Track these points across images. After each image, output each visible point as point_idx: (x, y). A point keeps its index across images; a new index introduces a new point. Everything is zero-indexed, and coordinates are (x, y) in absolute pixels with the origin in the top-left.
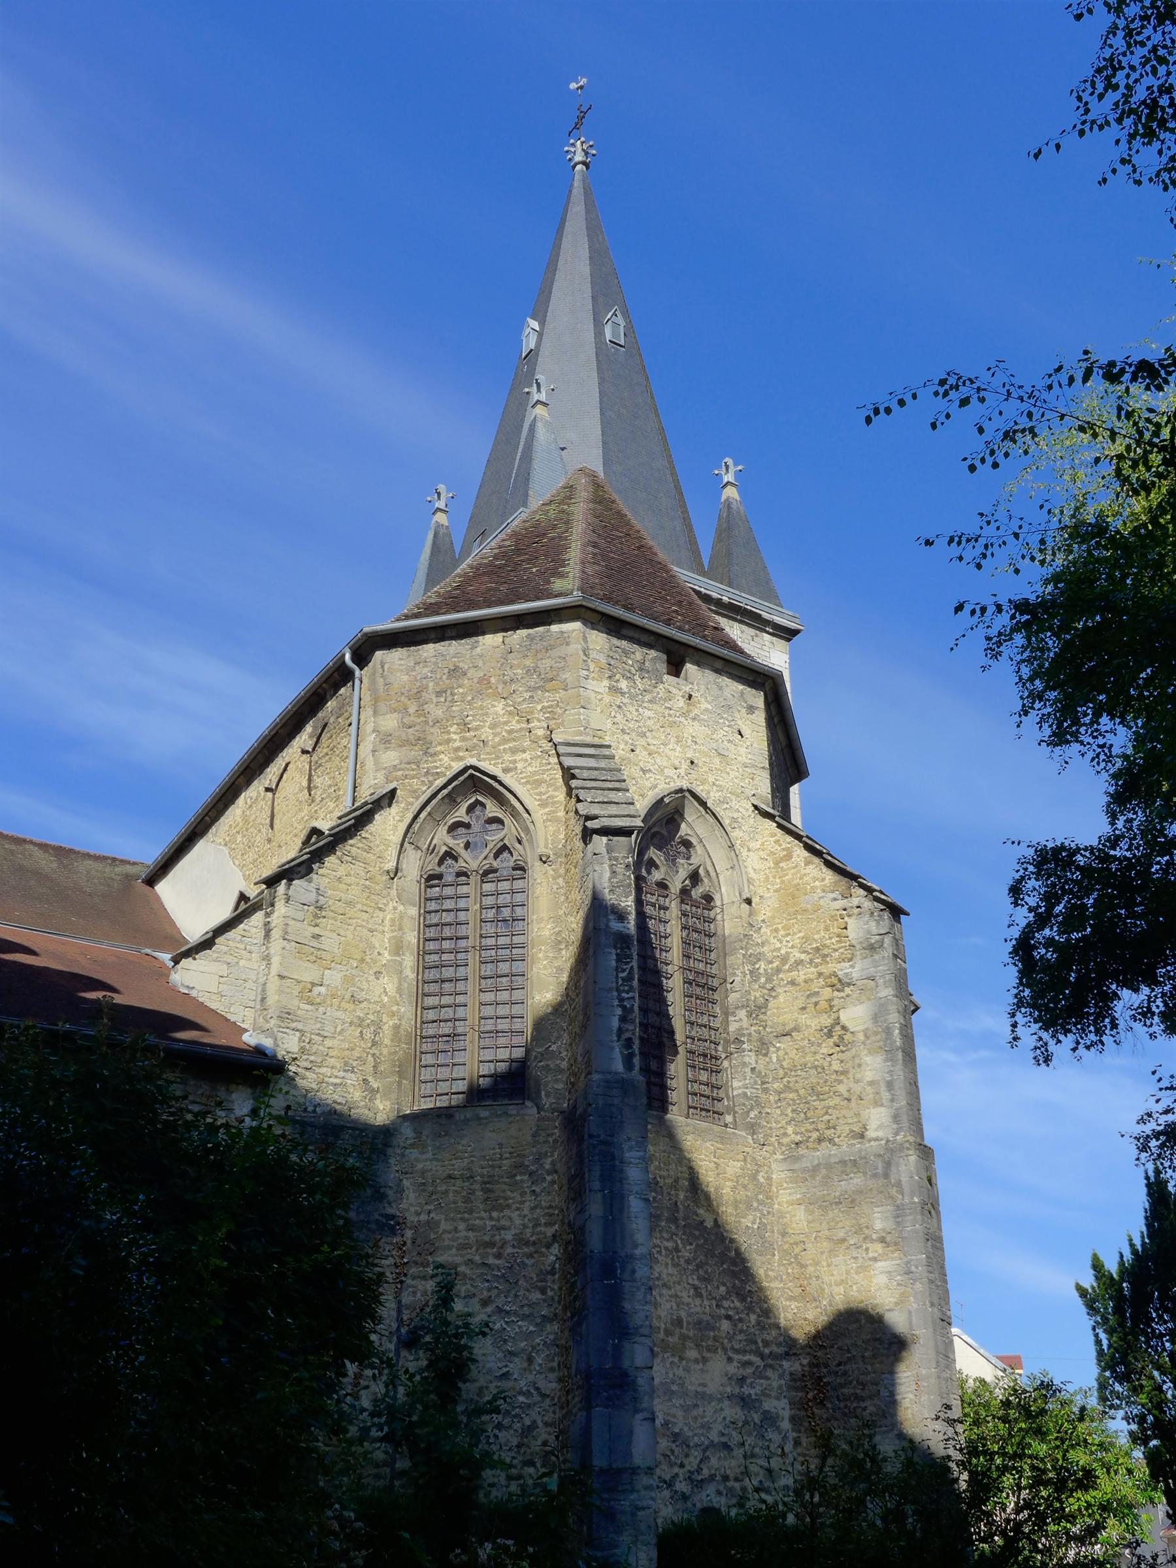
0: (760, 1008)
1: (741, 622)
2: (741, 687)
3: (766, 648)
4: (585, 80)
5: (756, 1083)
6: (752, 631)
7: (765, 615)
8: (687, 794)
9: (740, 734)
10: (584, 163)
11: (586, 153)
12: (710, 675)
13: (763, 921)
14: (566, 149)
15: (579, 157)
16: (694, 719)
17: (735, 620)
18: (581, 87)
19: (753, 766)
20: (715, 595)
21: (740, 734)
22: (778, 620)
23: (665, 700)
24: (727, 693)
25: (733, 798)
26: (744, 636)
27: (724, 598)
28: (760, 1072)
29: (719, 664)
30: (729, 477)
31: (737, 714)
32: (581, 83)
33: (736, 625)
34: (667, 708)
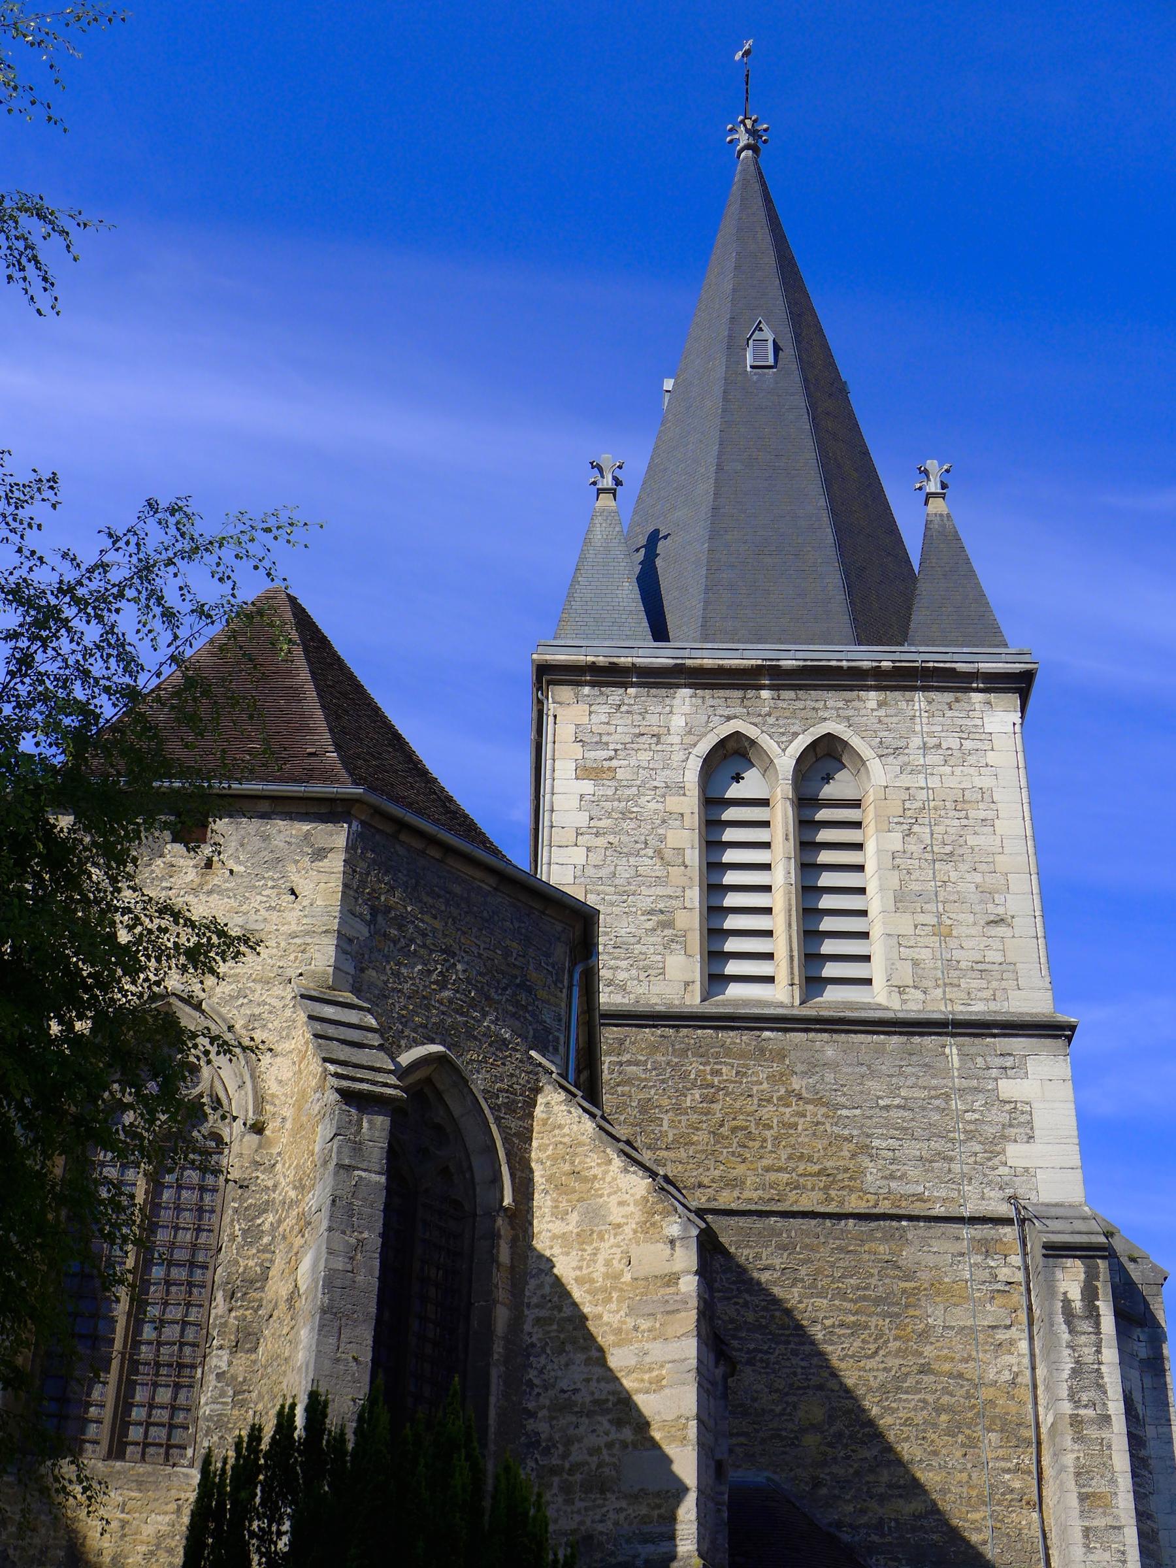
0: (252, 1282)
1: (924, 689)
2: (306, 827)
3: (977, 714)
4: (751, 42)
5: (223, 1394)
6: (949, 697)
7: (960, 667)
8: (173, 1000)
9: (293, 892)
10: (747, 147)
11: (753, 133)
12: (250, 826)
13: (279, 1154)
14: (728, 139)
15: (743, 139)
16: (210, 893)
17: (915, 689)
18: (747, 53)
19: (307, 933)
20: (866, 664)
21: (293, 892)
22: (985, 667)
23: (162, 879)
24: (278, 842)
25: (258, 987)
26: (933, 707)
27: (884, 664)
28: (234, 1377)
29: (264, 806)
30: (933, 486)
31: (292, 868)
32: (747, 47)
33: (919, 696)
34: (163, 889)
